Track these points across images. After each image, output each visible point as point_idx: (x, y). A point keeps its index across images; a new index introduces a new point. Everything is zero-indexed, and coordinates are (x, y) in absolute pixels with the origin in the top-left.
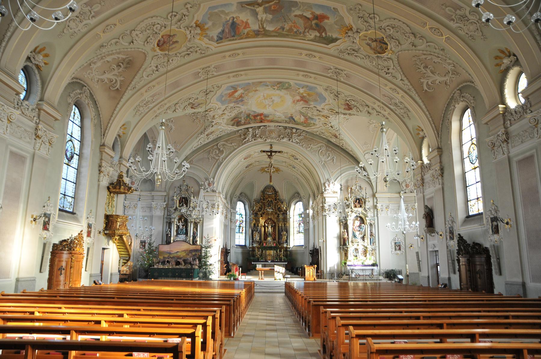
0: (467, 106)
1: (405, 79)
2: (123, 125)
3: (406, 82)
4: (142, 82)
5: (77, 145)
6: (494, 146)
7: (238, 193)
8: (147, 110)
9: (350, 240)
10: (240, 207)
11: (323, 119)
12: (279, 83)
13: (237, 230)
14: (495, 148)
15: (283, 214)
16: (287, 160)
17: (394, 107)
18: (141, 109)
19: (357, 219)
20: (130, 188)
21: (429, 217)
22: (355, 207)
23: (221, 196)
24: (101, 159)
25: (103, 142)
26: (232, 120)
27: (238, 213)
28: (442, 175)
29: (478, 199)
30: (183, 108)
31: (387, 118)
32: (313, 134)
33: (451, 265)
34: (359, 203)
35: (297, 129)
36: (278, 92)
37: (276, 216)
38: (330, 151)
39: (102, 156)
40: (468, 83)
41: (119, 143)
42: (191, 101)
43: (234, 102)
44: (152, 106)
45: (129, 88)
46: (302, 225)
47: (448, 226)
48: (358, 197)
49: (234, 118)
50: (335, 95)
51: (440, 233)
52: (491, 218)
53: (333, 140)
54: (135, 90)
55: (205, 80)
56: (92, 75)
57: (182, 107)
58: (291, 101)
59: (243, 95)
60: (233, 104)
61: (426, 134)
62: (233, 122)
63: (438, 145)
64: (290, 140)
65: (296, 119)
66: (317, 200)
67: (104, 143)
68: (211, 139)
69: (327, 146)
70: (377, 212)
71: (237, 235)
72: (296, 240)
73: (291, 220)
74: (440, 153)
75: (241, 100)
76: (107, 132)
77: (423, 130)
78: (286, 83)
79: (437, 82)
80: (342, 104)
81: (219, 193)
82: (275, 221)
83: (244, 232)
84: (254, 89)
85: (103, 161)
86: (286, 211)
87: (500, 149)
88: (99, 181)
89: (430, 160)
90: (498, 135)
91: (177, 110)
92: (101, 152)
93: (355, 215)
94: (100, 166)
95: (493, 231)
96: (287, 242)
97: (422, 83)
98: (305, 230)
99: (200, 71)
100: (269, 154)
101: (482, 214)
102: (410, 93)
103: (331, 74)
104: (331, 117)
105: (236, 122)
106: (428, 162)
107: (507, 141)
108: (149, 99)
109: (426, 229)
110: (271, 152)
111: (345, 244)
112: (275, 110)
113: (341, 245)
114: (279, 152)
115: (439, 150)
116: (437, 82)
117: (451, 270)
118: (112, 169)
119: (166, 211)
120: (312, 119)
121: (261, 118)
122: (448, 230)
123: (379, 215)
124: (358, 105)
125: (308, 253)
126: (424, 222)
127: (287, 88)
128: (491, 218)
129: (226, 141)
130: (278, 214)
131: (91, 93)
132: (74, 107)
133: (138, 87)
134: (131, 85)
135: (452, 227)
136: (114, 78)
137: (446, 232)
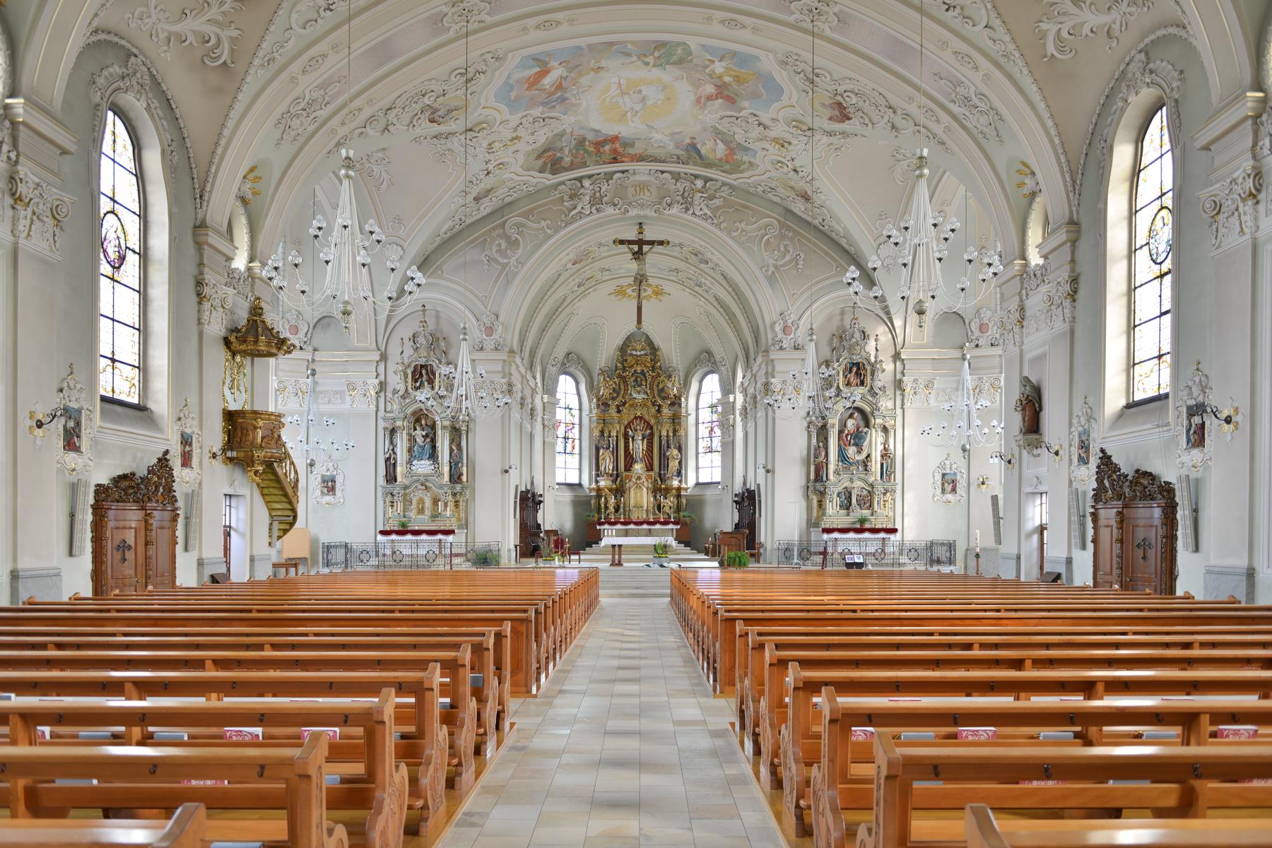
0: (1161, 98)
1: (997, 23)
2: (252, 170)
3: (1001, 32)
4: (291, 43)
5: (132, 224)
6: (1218, 213)
7: (560, 353)
8: (313, 127)
9: (832, 468)
10: (566, 386)
11: (773, 150)
12: (661, 45)
13: (560, 447)
14: (1221, 217)
15: (673, 404)
16: (682, 265)
17: (963, 110)
18: (296, 123)
19: (851, 416)
20: (283, 341)
21: (1031, 409)
22: (848, 384)
23: (518, 360)
24: (201, 264)
25: (200, 216)
26: (539, 157)
27: (562, 404)
28: (1073, 295)
29: (1160, 357)
30: (406, 122)
31: (943, 143)
32: (748, 192)
33: (1075, 526)
34: (858, 374)
35: (707, 180)
36: (656, 72)
37: (653, 410)
38: (791, 239)
39: (201, 256)
40: (1171, 30)
41: (243, 220)
42: (427, 101)
43: (544, 104)
44: (323, 113)
45: (256, 62)
46: (718, 431)
47: (1077, 429)
48: (856, 359)
49: (545, 151)
50: (808, 79)
51: (1056, 448)
52: (1189, 408)
53: (799, 207)
54: (273, 68)
55: (458, 39)
56: (150, 21)
57: (406, 118)
58: (692, 98)
59: (565, 84)
60: (541, 109)
61: (1042, 185)
62: (541, 162)
63: (1071, 212)
64: (687, 209)
65: (703, 152)
66: (755, 368)
67: (204, 221)
68: (488, 210)
69: (782, 225)
70: (903, 396)
71: (560, 459)
72: (703, 467)
73: (692, 420)
74: (1072, 236)
75: (559, 97)
76: (208, 189)
77: (1033, 173)
78: (679, 44)
79: (1086, 30)
80: (823, 105)
81: (512, 352)
82: (652, 421)
83: (577, 450)
84: (593, 64)
85: (206, 270)
86: (678, 397)
87: (1234, 220)
88: (199, 322)
89: (1045, 257)
90: (1234, 181)
91: (391, 128)
92: (199, 246)
94: (199, 283)
95: (1188, 441)
96: (679, 474)
97: (1043, 35)
98: (724, 445)
99: (445, 9)
100: (636, 248)
101: (1166, 396)
102: (1008, 66)
103: (797, 16)
104: (794, 142)
105: (551, 161)
106: (1041, 262)
107: (1254, 196)
108: (315, 95)
109: (1020, 437)
110: (641, 243)
111: (818, 478)
112: (650, 127)
114: (661, 243)
115: (1073, 228)
116: (1086, 30)
117: (1076, 540)
118: (231, 291)
119: (382, 401)
120: (746, 149)
121: (613, 150)
122: (1076, 442)
123: (907, 404)
124: (866, 106)
125: (730, 502)
126: (1017, 420)
127: (680, 62)
128: (1189, 408)
129: (525, 215)
130: (660, 406)
131: (152, 77)
132: (110, 114)
133: (280, 60)
134: (261, 54)
135: (1087, 433)
136: (209, 30)
137: (1070, 445)
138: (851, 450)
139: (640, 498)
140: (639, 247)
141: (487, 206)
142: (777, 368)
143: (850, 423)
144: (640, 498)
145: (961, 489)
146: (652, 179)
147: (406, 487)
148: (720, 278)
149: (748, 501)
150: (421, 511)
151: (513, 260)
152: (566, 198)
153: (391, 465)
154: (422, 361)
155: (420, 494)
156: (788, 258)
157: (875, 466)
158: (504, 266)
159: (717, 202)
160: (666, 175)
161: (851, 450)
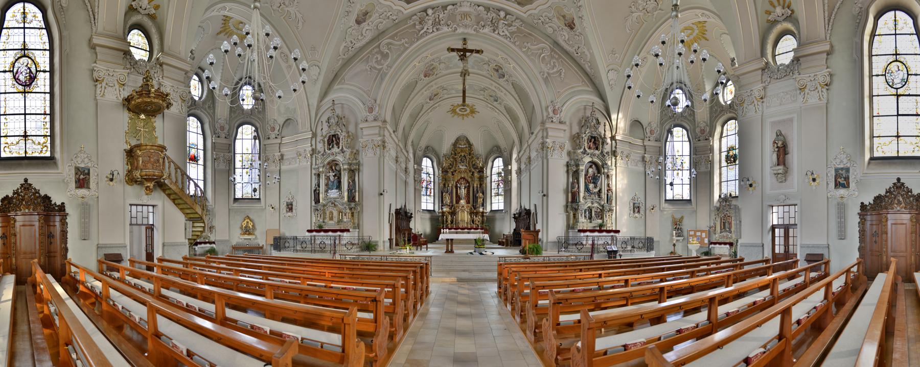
19: (591, 167)
35: (507, 13)
38: (557, 59)
64: (494, 31)
69: (552, 50)
93: (590, 160)
110: (465, 50)
113: (567, 202)
114: (478, 52)
129: (392, 37)
138: (591, 186)
139: (464, 216)
140: (464, 53)
141: (368, 30)
142: (550, 134)
143: (590, 170)
144: (464, 216)
145: (642, 212)
146: (472, 10)
147: (324, 206)
148: (510, 88)
149: (524, 218)
150: (331, 219)
151: (385, 66)
152: (417, 23)
153: (316, 194)
154: (332, 133)
155: (330, 209)
156: (555, 70)
157: (604, 196)
158: (380, 70)
159: (513, 29)
160: (481, 8)
161: (591, 186)
